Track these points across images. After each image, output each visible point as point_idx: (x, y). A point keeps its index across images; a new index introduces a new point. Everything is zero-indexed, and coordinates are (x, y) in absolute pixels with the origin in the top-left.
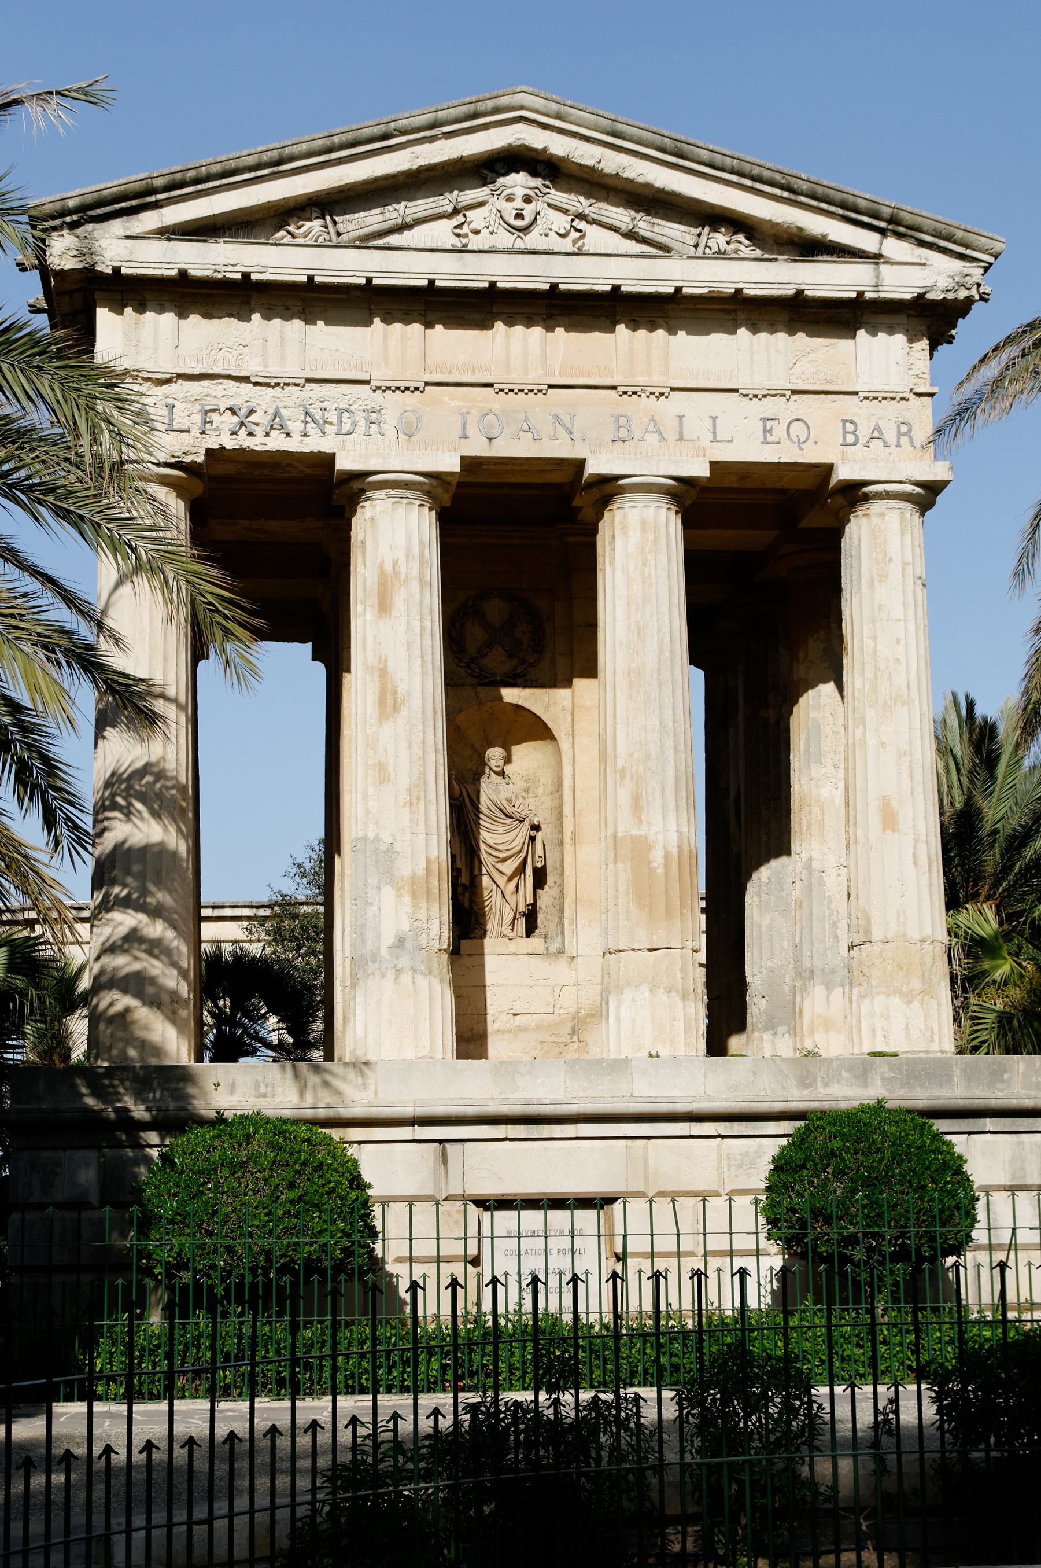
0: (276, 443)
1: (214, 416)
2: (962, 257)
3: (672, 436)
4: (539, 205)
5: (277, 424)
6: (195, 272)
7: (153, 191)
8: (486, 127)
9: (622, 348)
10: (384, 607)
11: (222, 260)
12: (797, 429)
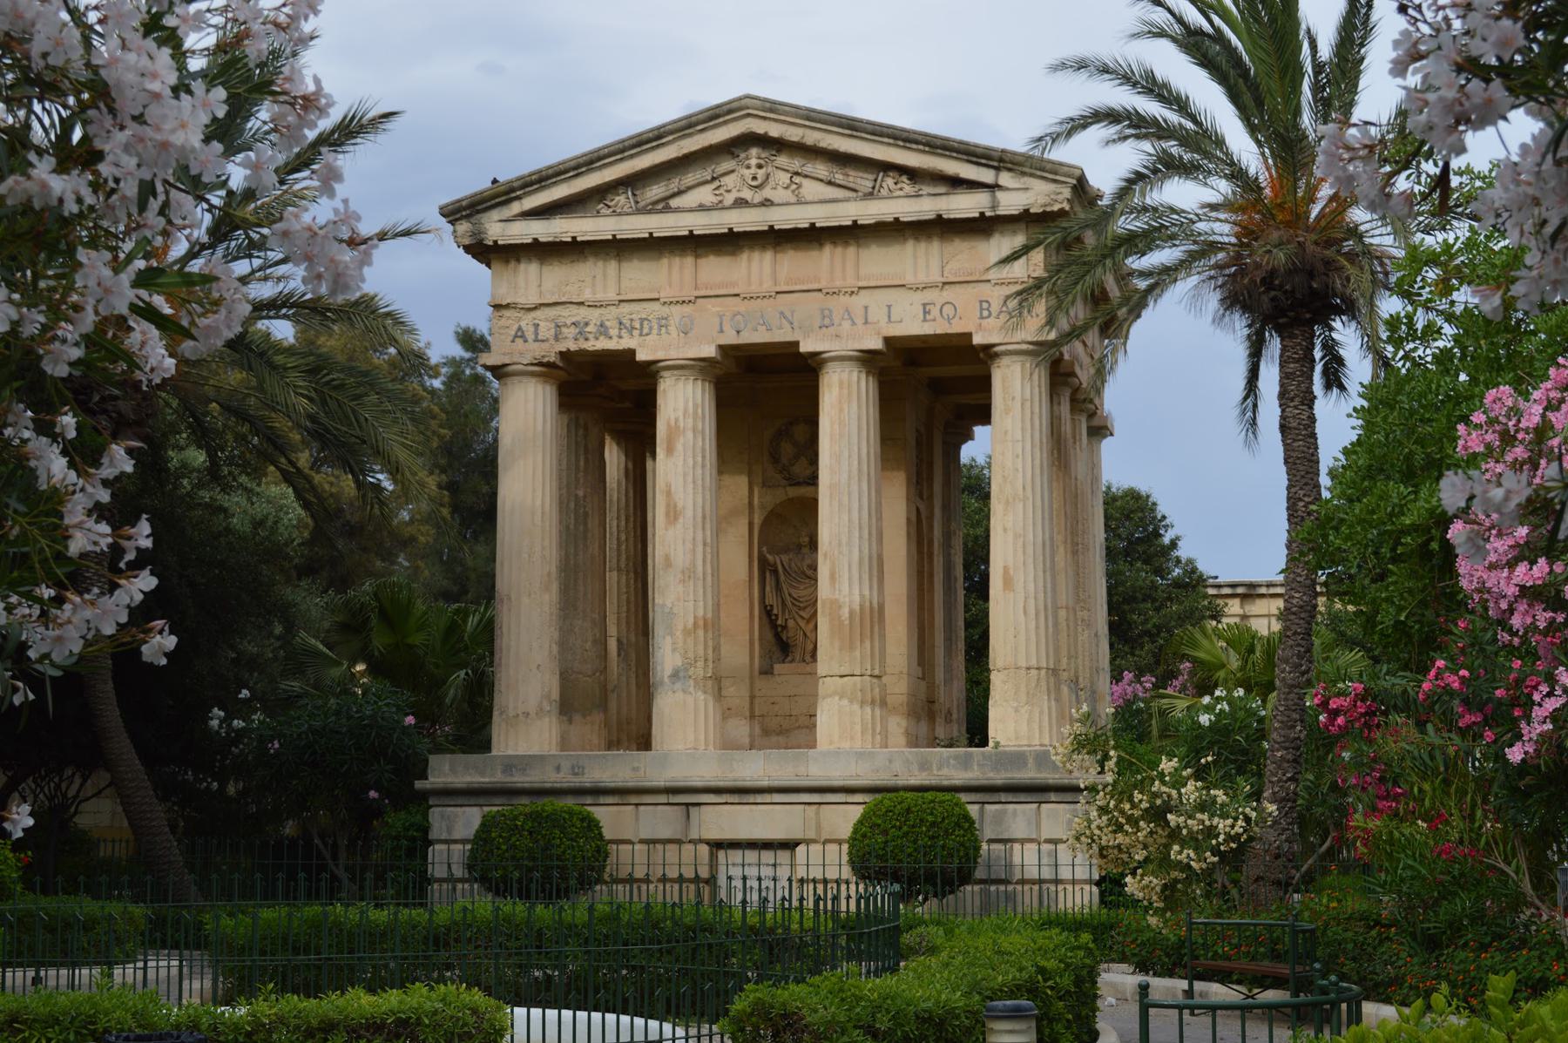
1: (564, 330)
2: (1055, 181)
3: (859, 321)
5: (603, 330)
7: (513, 190)
8: (725, 123)
9: (825, 263)
10: (670, 450)
11: (558, 230)
12: (948, 310)
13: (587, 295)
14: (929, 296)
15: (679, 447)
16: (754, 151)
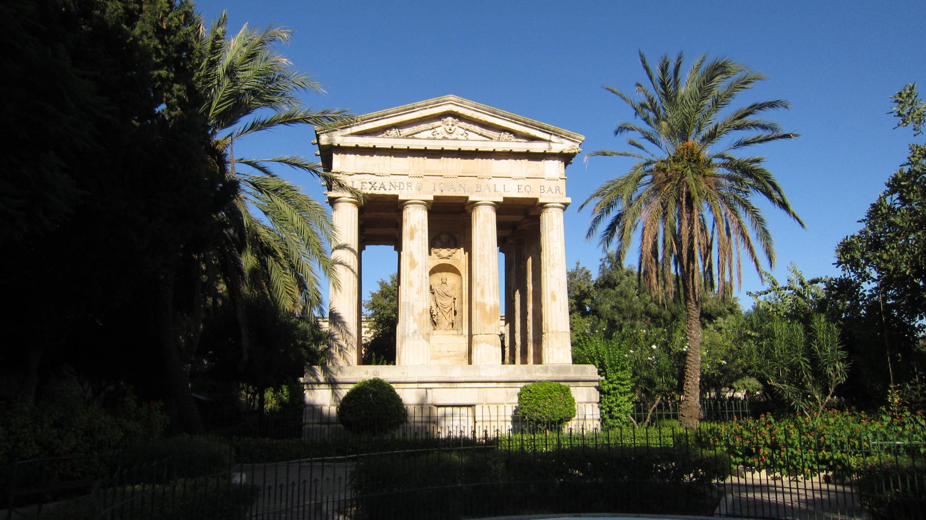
0: (382, 192)
3: (493, 190)
4: (456, 127)
6: (360, 145)
10: (412, 237)
12: (528, 188)
13: (376, 171)
14: (520, 182)
15: (416, 236)
16: (450, 119)
